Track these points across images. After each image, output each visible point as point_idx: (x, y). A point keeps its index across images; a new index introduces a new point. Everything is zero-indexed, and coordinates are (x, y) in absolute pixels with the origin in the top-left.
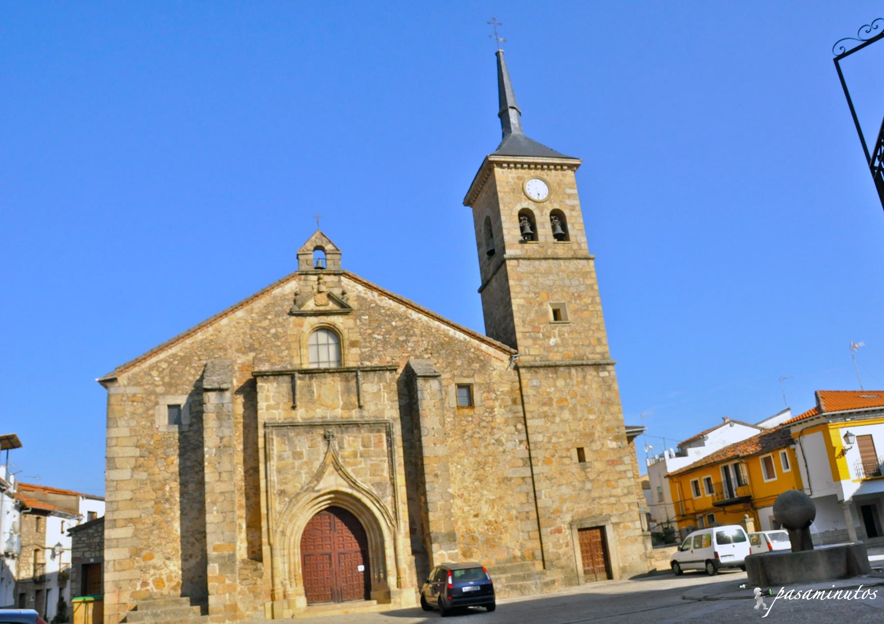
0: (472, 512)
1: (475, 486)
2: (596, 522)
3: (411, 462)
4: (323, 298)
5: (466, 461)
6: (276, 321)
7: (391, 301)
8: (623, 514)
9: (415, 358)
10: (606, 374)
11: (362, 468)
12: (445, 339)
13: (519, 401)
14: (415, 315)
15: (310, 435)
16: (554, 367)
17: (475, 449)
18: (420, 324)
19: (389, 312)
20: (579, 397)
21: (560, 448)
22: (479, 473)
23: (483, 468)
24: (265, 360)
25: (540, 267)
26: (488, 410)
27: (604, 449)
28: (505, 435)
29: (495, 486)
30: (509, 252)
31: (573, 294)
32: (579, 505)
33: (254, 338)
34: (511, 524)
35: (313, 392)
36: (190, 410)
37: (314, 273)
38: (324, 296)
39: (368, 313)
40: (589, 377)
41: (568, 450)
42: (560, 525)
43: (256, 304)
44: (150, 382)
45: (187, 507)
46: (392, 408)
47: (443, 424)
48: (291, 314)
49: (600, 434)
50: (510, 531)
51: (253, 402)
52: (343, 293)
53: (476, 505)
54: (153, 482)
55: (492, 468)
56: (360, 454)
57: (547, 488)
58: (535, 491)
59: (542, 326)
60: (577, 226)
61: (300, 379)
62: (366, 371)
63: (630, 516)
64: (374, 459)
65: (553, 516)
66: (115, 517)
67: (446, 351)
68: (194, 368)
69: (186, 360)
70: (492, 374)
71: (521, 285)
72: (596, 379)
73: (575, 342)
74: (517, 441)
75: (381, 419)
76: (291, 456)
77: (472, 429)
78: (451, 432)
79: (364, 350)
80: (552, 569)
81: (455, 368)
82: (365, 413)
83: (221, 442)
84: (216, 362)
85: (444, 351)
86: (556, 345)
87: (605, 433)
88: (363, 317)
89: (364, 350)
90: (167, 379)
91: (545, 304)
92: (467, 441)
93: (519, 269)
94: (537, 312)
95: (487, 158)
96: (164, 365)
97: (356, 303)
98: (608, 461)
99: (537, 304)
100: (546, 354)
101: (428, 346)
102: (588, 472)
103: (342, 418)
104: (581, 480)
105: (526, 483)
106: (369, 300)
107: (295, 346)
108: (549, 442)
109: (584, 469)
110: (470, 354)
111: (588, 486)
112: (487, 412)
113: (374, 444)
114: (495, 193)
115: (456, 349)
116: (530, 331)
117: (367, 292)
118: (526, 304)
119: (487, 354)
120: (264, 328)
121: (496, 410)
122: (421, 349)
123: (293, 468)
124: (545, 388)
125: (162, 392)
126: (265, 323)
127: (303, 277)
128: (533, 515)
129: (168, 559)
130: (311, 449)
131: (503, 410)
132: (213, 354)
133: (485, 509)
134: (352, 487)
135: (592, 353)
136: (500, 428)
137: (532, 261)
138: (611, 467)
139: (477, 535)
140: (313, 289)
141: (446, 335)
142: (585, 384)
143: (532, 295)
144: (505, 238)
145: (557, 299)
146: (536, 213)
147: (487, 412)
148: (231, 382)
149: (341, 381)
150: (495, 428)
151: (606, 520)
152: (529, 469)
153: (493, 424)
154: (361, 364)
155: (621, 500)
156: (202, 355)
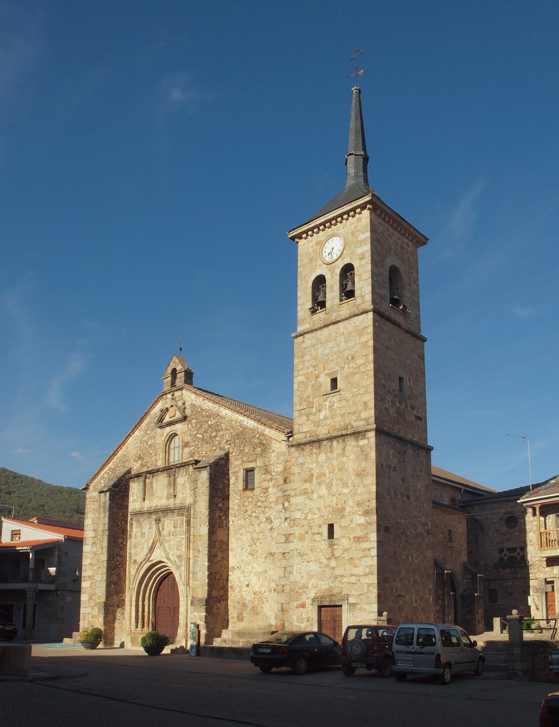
10: (365, 442)
15: (149, 520)
16: (319, 441)
17: (251, 527)
19: (207, 414)
20: (336, 471)
21: (314, 525)
22: (253, 548)
23: (255, 544)
25: (322, 337)
27: (352, 526)
28: (274, 513)
29: (263, 560)
31: (347, 359)
32: (323, 582)
34: (270, 596)
40: (348, 448)
42: (305, 600)
46: (191, 496)
50: (269, 601)
53: (248, 576)
56: (172, 533)
59: (315, 400)
60: (364, 277)
63: (368, 598)
64: (178, 537)
65: (300, 591)
67: (240, 440)
72: (355, 449)
73: (342, 412)
74: (283, 518)
78: (237, 513)
81: (245, 454)
85: (238, 441)
86: (325, 418)
87: (356, 508)
88: (193, 421)
91: (321, 376)
92: (247, 520)
93: (304, 345)
94: (313, 386)
97: (189, 410)
98: (355, 538)
100: (315, 429)
102: (334, 549)
104: (327, 558)
106: (197, 406)
108: (305, 519)
109: (331, 546)
111: (333, 563)
118: (305, 380)
119: (269, 437)
121: (269, 489)
124: (308, 465)
131: (276, 489)
133: (254, 580)
135: (357, 420)
136: (271, 507)
137: (315, 332)
138: (357, 544)
139: (246, 602)
141: (241, 426)
149: (167, 477)
150: (266, 507)
151: (343, 600)
153: (265, 504)
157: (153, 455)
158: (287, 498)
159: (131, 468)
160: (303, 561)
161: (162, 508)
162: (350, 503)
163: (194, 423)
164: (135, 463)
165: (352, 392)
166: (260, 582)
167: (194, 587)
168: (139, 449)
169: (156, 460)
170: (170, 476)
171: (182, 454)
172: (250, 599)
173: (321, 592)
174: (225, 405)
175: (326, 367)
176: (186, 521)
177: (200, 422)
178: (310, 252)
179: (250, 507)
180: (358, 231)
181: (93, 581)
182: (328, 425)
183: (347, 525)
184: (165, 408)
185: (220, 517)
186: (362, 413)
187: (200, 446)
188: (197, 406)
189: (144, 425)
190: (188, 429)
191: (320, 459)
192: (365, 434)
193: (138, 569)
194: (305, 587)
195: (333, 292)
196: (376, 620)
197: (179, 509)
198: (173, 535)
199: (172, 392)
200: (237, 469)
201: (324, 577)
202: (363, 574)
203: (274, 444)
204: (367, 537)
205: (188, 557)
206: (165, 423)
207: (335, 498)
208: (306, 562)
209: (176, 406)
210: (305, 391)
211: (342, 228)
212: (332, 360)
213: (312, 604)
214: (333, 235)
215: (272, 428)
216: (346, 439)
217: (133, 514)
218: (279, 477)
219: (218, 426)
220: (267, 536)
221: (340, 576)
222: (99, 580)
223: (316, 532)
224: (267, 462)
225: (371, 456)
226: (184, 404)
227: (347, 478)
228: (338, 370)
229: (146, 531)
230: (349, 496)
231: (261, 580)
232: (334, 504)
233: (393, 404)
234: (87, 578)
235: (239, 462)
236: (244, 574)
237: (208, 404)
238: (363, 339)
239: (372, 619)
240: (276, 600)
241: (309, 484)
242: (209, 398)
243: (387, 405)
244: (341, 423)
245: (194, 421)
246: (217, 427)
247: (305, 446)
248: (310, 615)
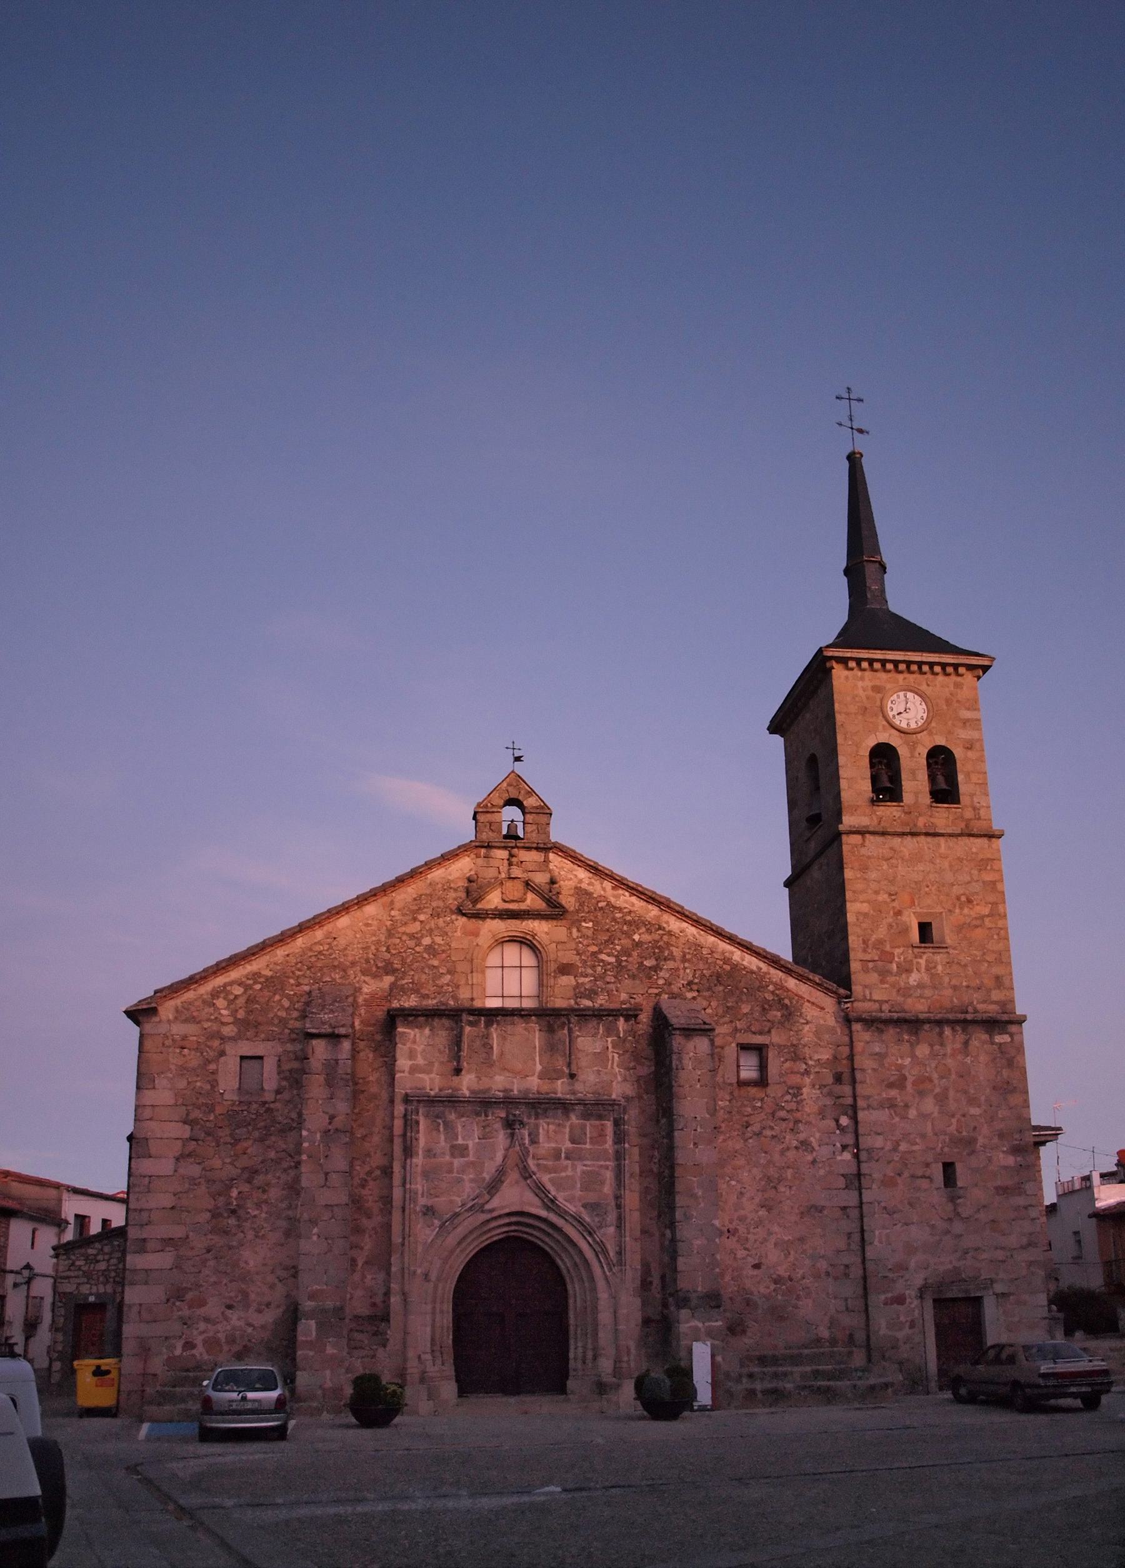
0: (750, 1259)
1: (759, 1217)
2: (967, 1291)
3: (651, 1171)
4: (514, 889)
6: (433, 926)
7: (634, 899)
8: (1016, 1279)
9: (669, 998)
10: (1006, 1038)
12: (724, 966)
13: (846, 1077)
14: (674, 924)
19: (628, 918)
20: (953, 1076)
21: (912, 1161)
22: (766, 1196)
23: (775, 1188)
25: (902, 849)
26: (790, 1091)
28: (818, 1135)
30: (848, 821)
31: (958, 898)
33: (394, 952)
34: (816, 1285)
35: (492, 1048)
36: (279, 1066)
37: (503, 845)
38: (519, 886)
40: (975, 1043)
41: (927, 1165)
43: (399, 894)
44: (213, 1017)
45: (265, 1225)
46: (625, 1080)
47: (713, 1112)
48: (460, 912)
51: (386, 1059)
52: (553, 882)
54: (210, 1181)
55: (790, 1187)
57: (884, 1227)
58: (862, 1231)
59: (897, 951)
61: (471, 1024)
62: (584, 1015)
65: (891, 1275)
66: (144, 1236)
68: (288, 997)
69: (274, 983)
71: (865, 879)
73: (954, 982)
74: (838, 1145)
75: (606, 1097)
76: (448, 1152)
77: (761, 1122)
78: (723, 1125)
79: (581, 980)
81: (739, 1017)
82: (579, 1087)
83: (330, 1123)
84: (326, 989)
85: (721, 988)
86: (921, 986)
87: (996, 1140)
88: (584, 924)
89: (581, 980)
90: (241, 1014)
91: (906, 913)
92: (750, 1141)
93: (863, 851)
94: (890, 926)
95: (820, 650)
96: (238, 990)
97: (573, 900)
98: (997, 1188)
99: (892, 913)
100: (900, 999)
101: (694, 976)
103: (539, 1093)
104: (946, 1218)
105: (848, 1217)
106: (595, 896)
107: (462, 967)
108: (895, 1149)
109: (953, 1199)
110: (766, 995)
111: (958, 1227)
112: (790, 1094)
113: (591, 1138)
114: (831, 716)
115: (742, 984)
116: (876, 958)
117: (593, 881)
118: (872, 912)
119: (796, 995)
120: (412, 936)
121: (805, 1090)
122: (682, 982)
123: (450, 1171)
125: (233, 1034)
126: (415, 927)
127: (483, 851)
128: (856, 1272)
129: (229, 1307)
130: (483, 1141)
131: (818, 1092)
132: (322, 975)
133: (773, 1256)
134: (548, 1208)
135: (984, 1002)
140: (499, 873)
141: (727, 961)
142: (968, 1056)
143: (883, 897)
144: (843, 794)
145: (929, 906)
146: (903, 751)
147: (790, 1094)
148: (353, 1026)
150: (801, 1121)
152: (856, 1193)
153: (798, 1115)
154: (576, 1003)
156: (303, 975)
162: (985, 1130)
182: (927, 998)
207: (954, 1121)
208: (900, 1224)
218: (824, 1070)
223: (920, 1174)
229: (470, 1144)
230: (983, 1120)
231: (792, 1256)
232: (953, 1128)
239: (1039, 1316)
244: (952, 1000)
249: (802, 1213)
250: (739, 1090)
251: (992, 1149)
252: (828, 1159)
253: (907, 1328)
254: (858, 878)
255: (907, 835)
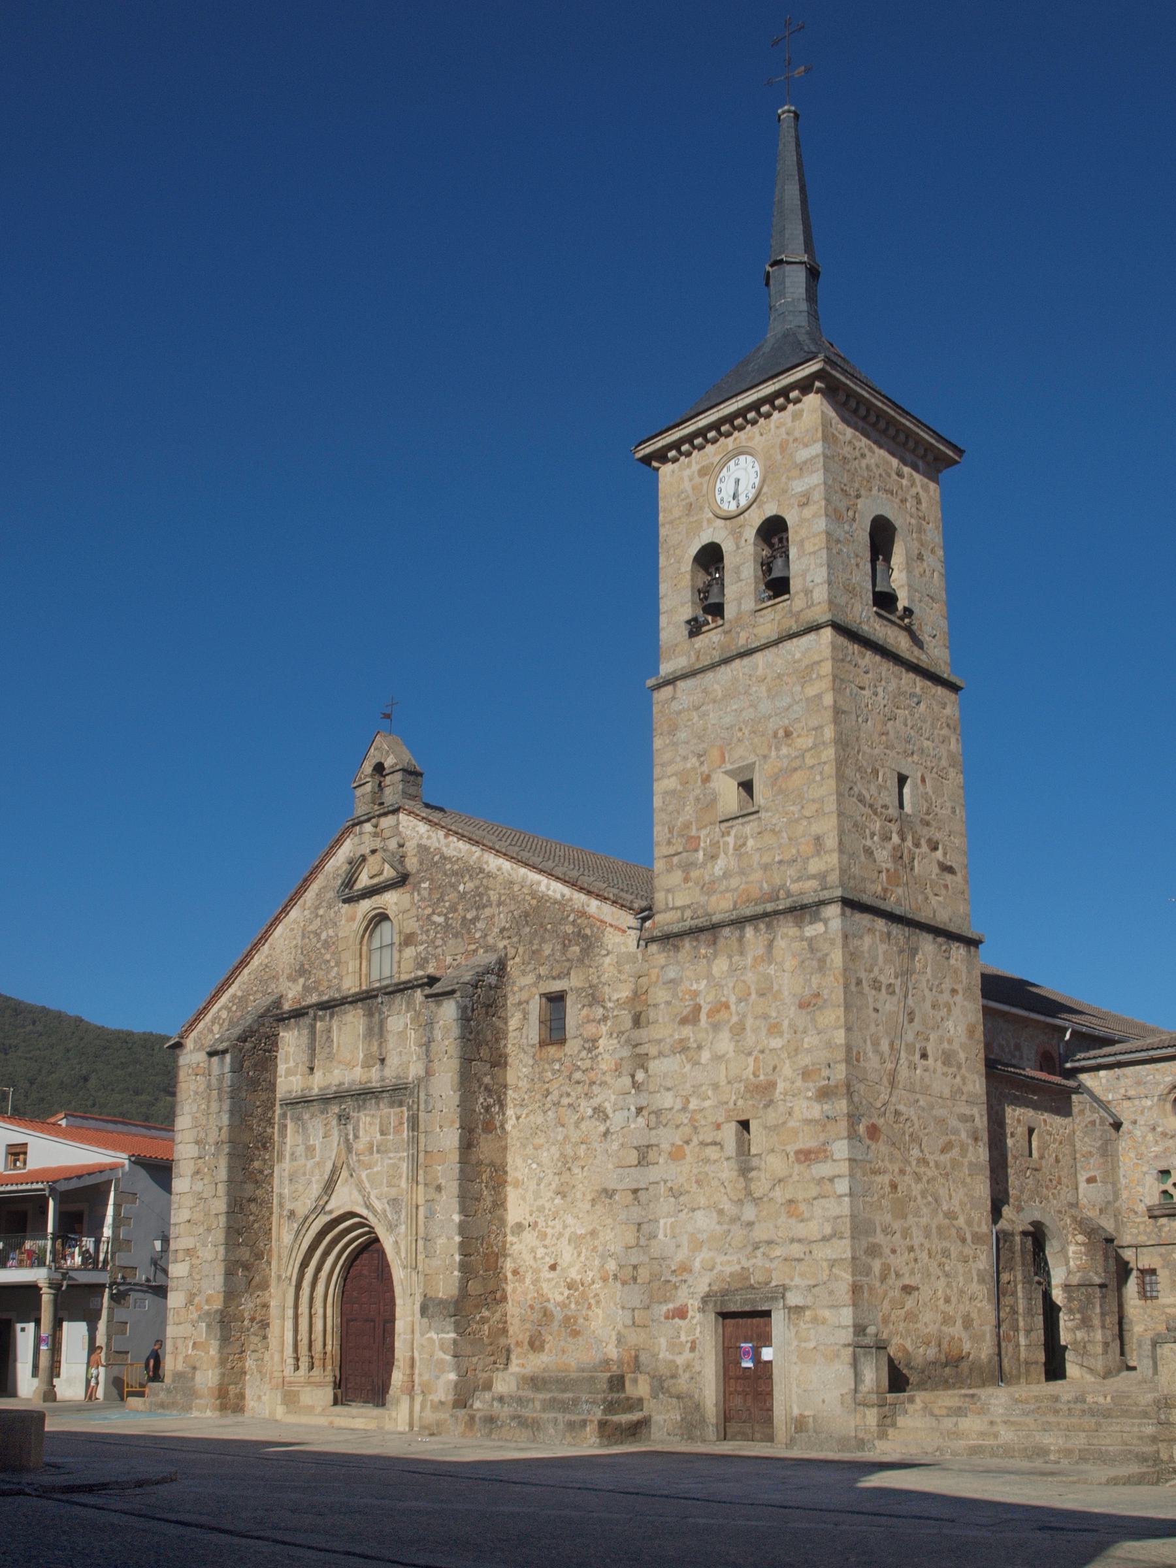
2: (753, 1301)
5: (545, 1154)
8: (814, 1286)
10: (819, 928)
11: (378, 1172)
15: (324, 1116)
16: (713, 928)
17: (560, 1129)
18: (500, 879)
19: (456, 867)
20: (754, 996)
21: (703, 1122)
24: (314, 988)
25: (716, 686)
26: (586, 1045)
27: (792, 1124)
28: (613, 1097)
29: (588, 1206)
31: (775, 735)
34: (606, 1291)
39: (428, 876)
40: (781, 943)
42: (686, 1300)
46: (419, 1059)
49: (788, 1085)
50: (603, 1304)
53: (554, 1245)
57: (669, 1215)
59: (703, 833)
60: (809, 547)
64: (391, 1155)
65: (673, 1279)
70: (602, 965)
72: (796, 945)
73: (766, 859)
74: (633, 1109)
78: (526, 1097)
80: (661, 1396)
81: (542, 961)
85: (527, 929)
86: (727, 875)
87: (799, 1083)
88: (423, 885)
91: (714, 776)
92: (550, 1113)
93: (675, 706)
94: (698, 799)
97: (415, 860)
98: (798, 1153)
102: (751, 1179)
103: (361, 1084)
108: (684, 1109)
109: (745, 1170)
111: (749, 1213)
112: (585, 1048)
116: (681, 849)
117: (431, 833)
118: (679, 787)
119: (598, 920)
121: (601, 1041)
131: (615, 1041)
133: (567, 1254)
135: (799, 879)
136: (606, 1083)
137: (699, 676)
138: (802, 1167)
139: (550, 1306)
141: (533, 894)
142: (770, 964)
150: (594, 1083)
151: (774, 1299)
153: (592, 1074)
155: (815, 1252)
157: (332, 964)
158: (641, 1061)
159: (281, 996)
160: (680, 1208)
161: (353, 1088)
163: (425, 888)
164: (290, 984)
165: (787, 813)
166: (582, 1258)
167: (429, 1272)
168: (299, 951)
169: (340, 977)
170: (370, 1014)
171: (399, 962)
172: (559, 1298)
173: (723, 1280)
174: (497, 847)
175: (727, 756)
176: (408, 1117)
177: (439, 887)
178: (686, 491)
179: (555, 1084)
180: (795, 440)
181: (196, 1261)
183: (780, 1122)
184: (358, 855)
185: (487, 1109)
186: (811, 861)
187: (439, 942)
188: (432, 850)
189: (310, 895)
190: (413, 903)
191: (715, 970)
192: (818, 910)
193: (298, 1231)
194: (685, 1268)
195: (740, 584)
196: (849, 1345)
197: (392, 1090)
198: (378, 1152)
199: (374, 817)
200: (524, 996)
201: (730, 1245)
202: (819, 1237)
203: (611, 936)
204: (825, 1151)
205: (414, 1203)
206: (358, 890)
207: (751, 1060)
209: (385, 850)
210: (679, 813)
211: (757, 434)
212: (739, 740)
213: (702, 1310)
214: (740, 452)
215: (605, 899)
216: (775, 922)
217: (287, 1104)
218: (623, 1012)
219: (480, 895)
220: (596, 1150)
221: (766, 1242)
222: (210, 1259)
223: (709, 1140)
224: (595, 977)
225: (832, 961)
226: (401, 846)
227: (778, 1012)
228: (754, 763)
230: (784, 1055)
231: (583, 1255)
233: (887, 838)
234: (180, 1255)
235: (529, 979)
236: (544, 1240)
237: (456, 844)
238: (811, 691)
240: (618, 1301)
241: (690, 1027)
242: (460, 831)
243: (869, 843)
244: (762, 886)
245: (426, 885)
246: (477, 899)
247: (682, 940)
248: (698, 1335)
249: (593, 1200)
250: (541, 1051)
251: (793, 1096)
252: (622, 1128)
253: (687, 1350)
254: (667, 745)
255: (719, 665)
